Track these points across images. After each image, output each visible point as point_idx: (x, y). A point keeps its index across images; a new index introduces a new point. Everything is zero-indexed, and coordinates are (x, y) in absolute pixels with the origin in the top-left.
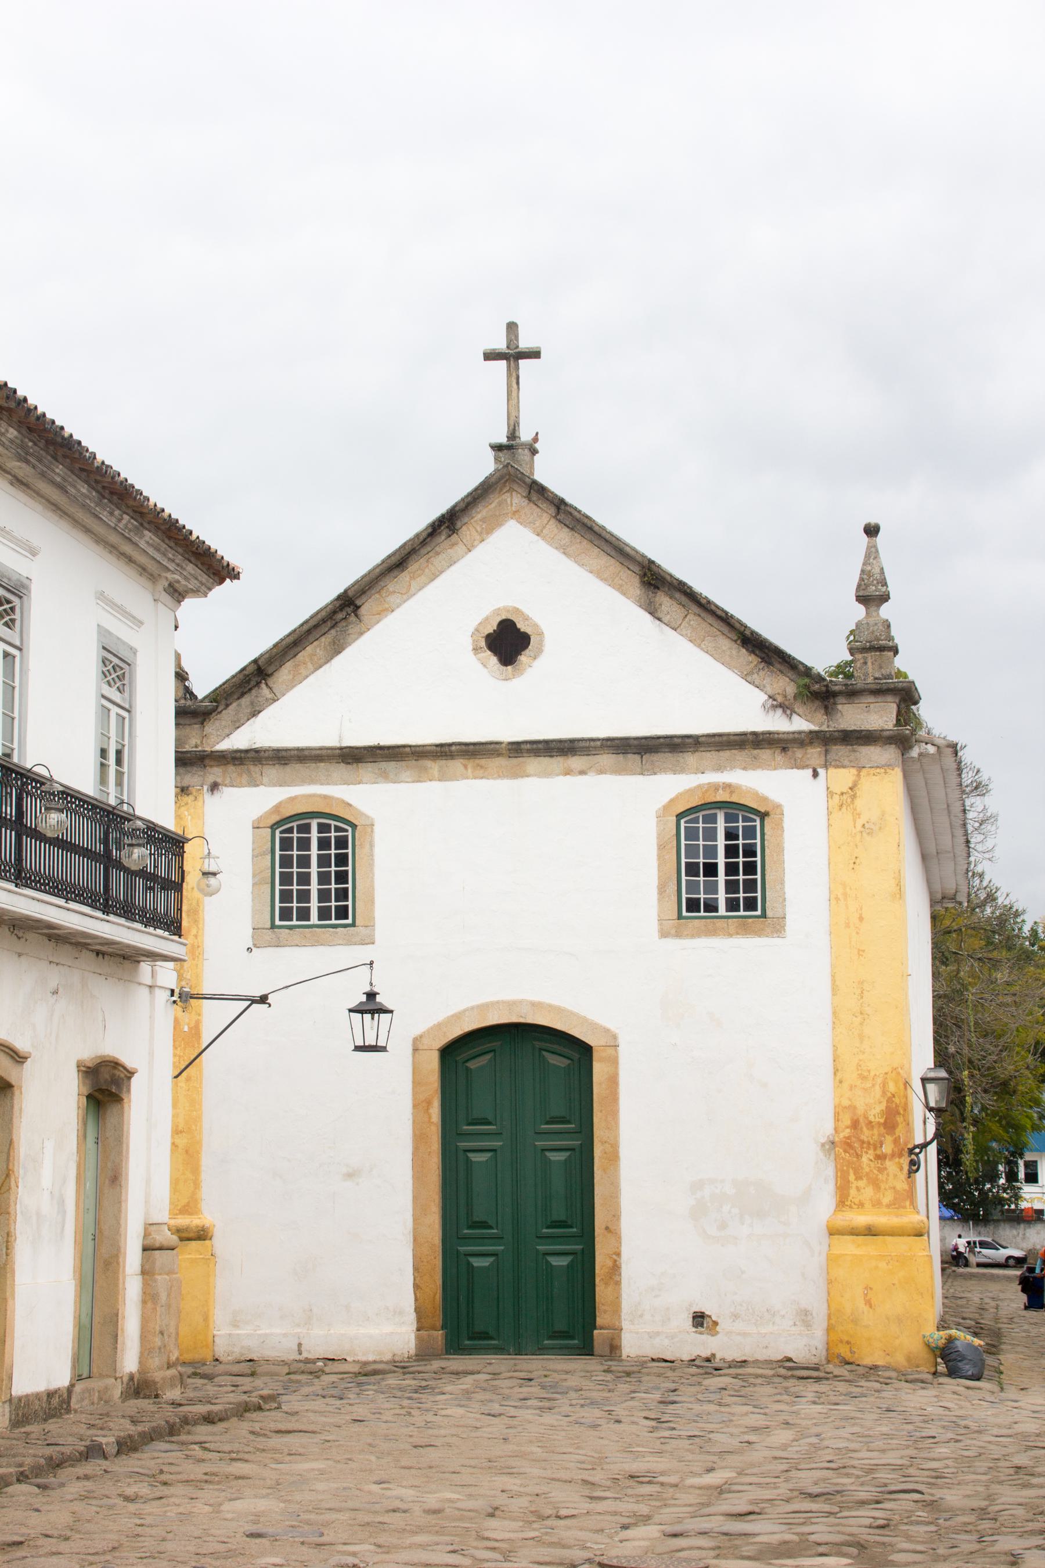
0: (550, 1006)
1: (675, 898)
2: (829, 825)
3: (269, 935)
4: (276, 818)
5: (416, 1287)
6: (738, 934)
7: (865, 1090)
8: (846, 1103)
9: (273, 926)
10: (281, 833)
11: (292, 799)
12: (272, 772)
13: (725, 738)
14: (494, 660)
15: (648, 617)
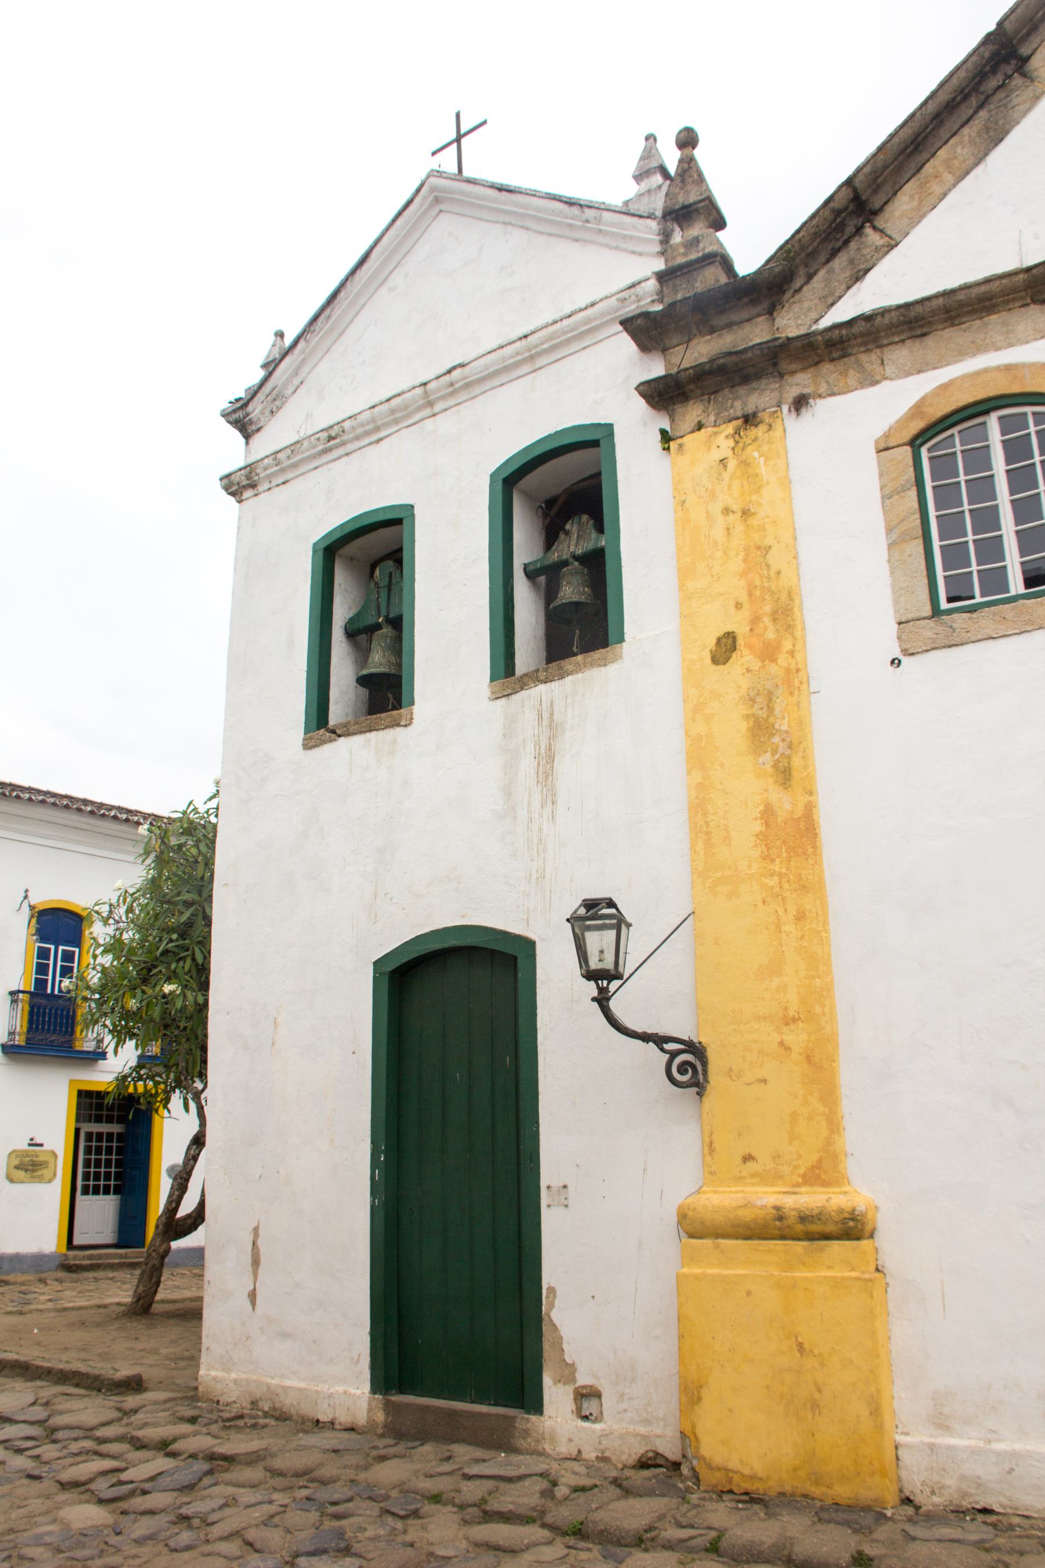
3: (930, 630)
9: (936, 612)
10: (929, 450)
11: (944, 387)
12: (900, 354)
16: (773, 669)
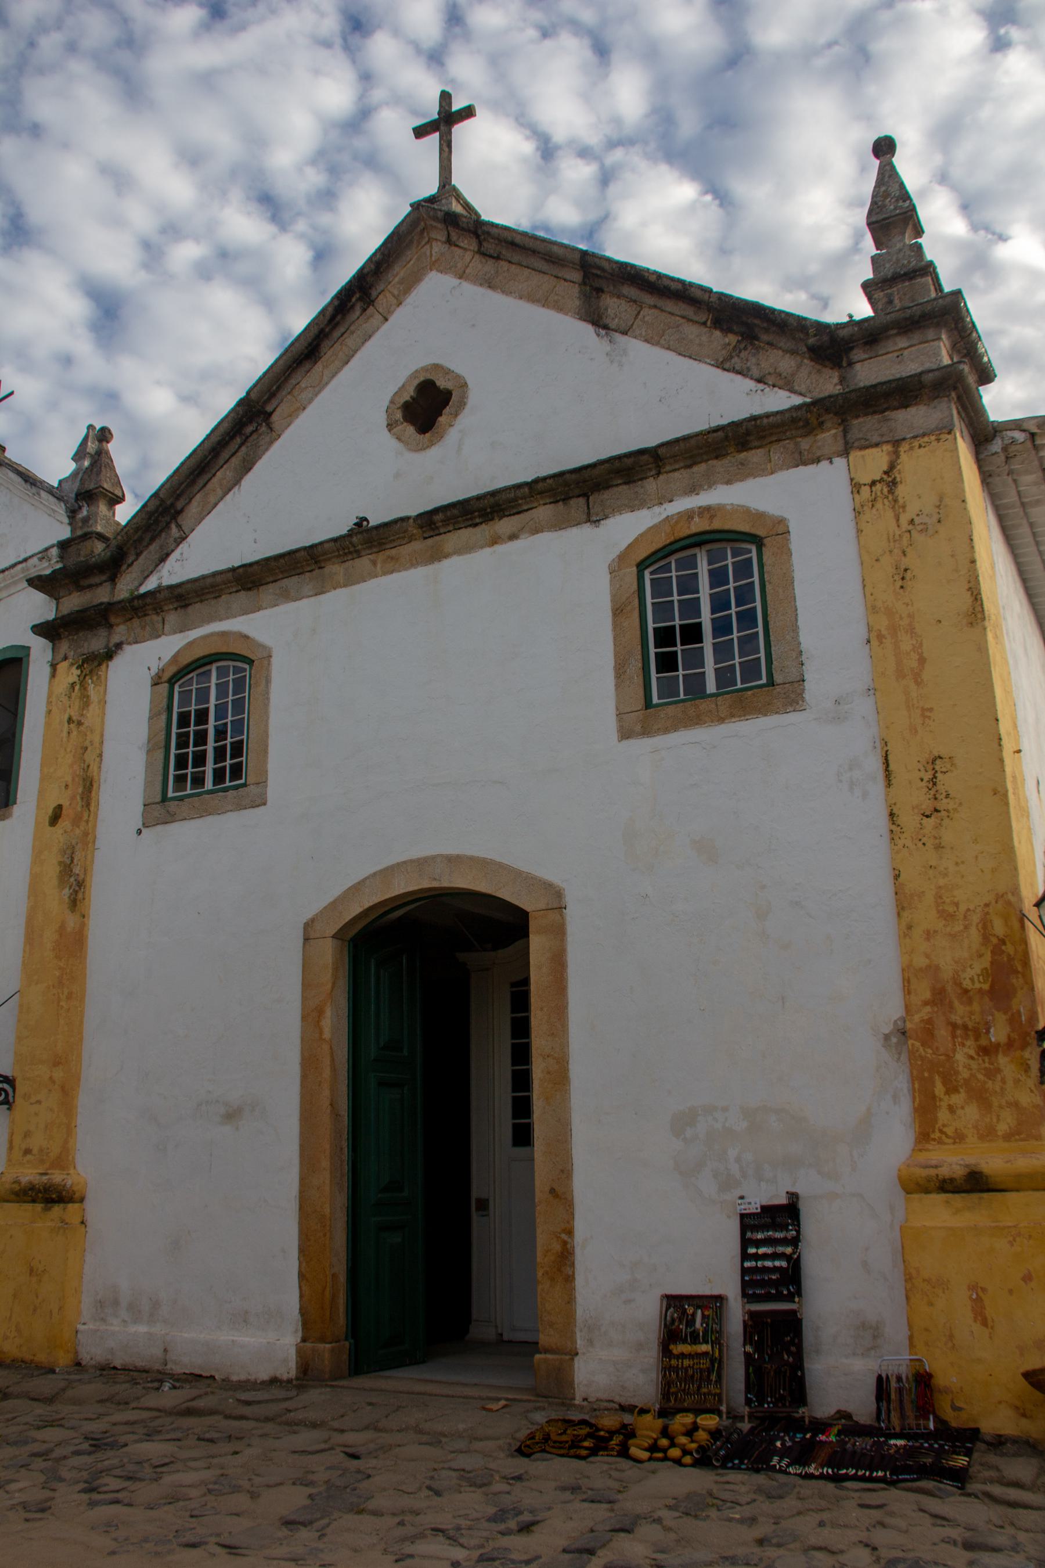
0: (472, 859)
1: (638, 680)
2: (859, 531)
4: (173, 669)
5: (301, 1276)
6: (732, 716)
7: (953, 936)
8: (921, 962)
9: (165, 799)
10: (180, 687)
11: (190, 644)
12: (172, 618)
13: (693, 442)
14: (410, 430)
15: (589, 328)
16: (77, 831)
